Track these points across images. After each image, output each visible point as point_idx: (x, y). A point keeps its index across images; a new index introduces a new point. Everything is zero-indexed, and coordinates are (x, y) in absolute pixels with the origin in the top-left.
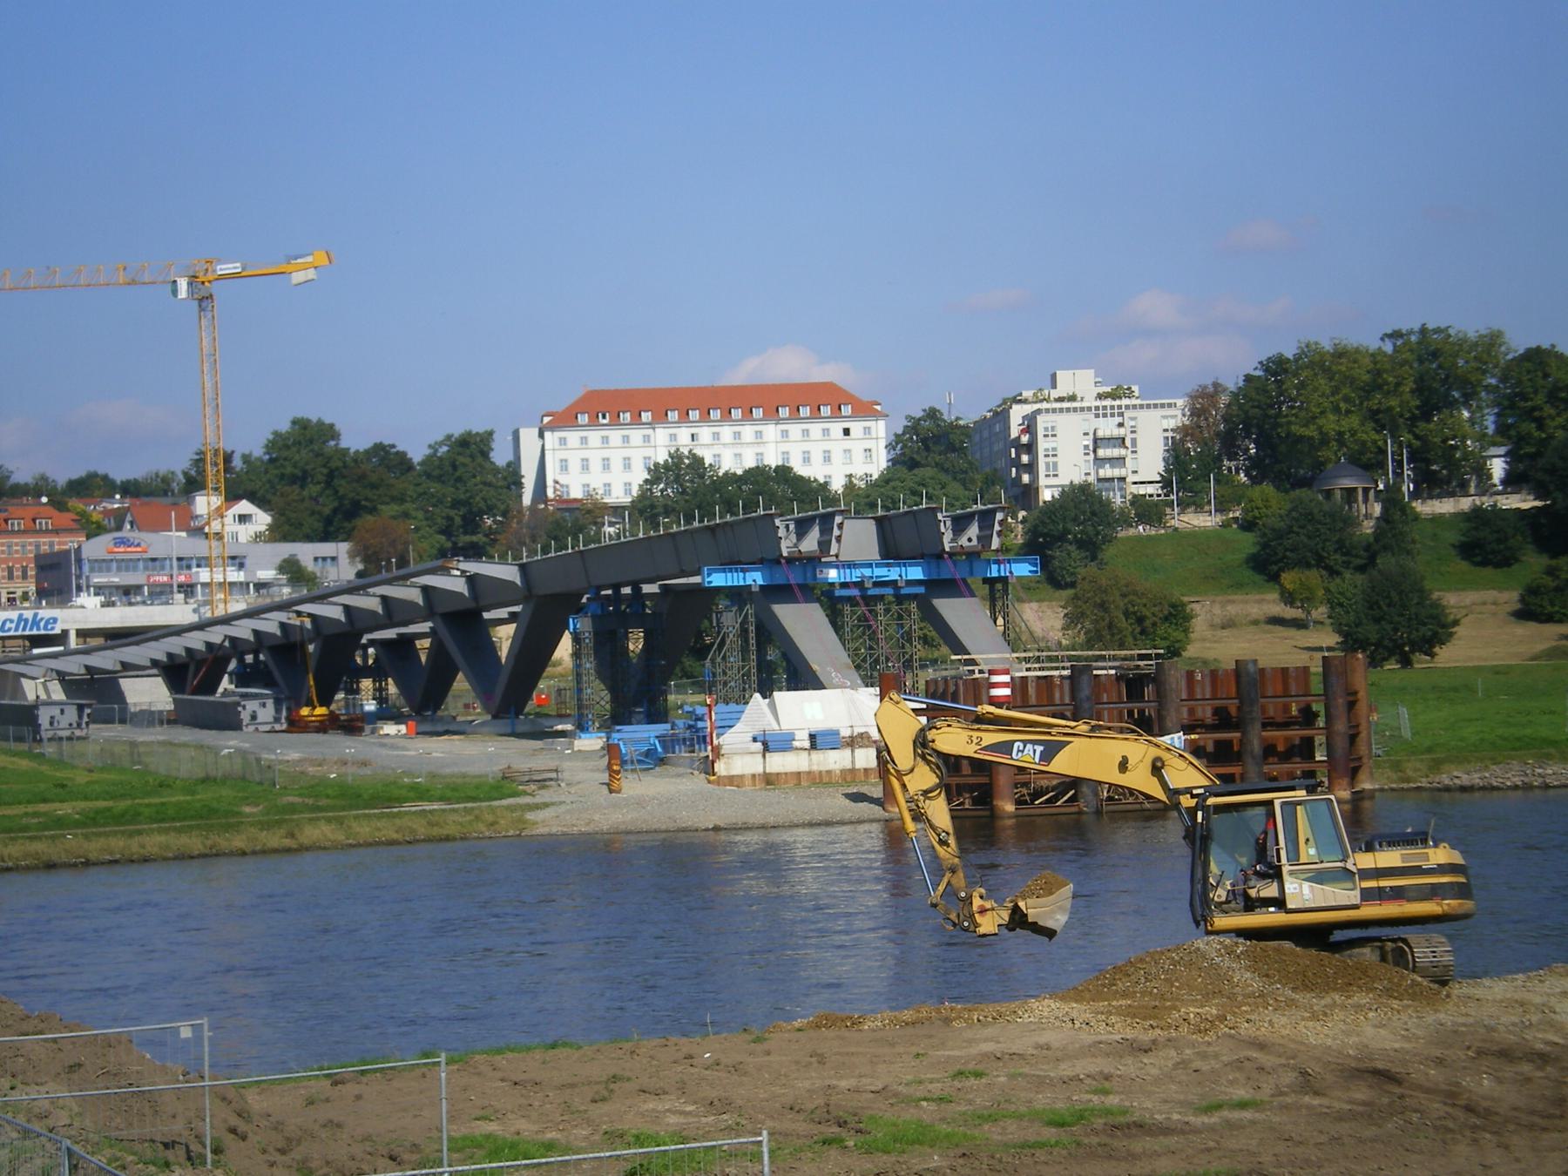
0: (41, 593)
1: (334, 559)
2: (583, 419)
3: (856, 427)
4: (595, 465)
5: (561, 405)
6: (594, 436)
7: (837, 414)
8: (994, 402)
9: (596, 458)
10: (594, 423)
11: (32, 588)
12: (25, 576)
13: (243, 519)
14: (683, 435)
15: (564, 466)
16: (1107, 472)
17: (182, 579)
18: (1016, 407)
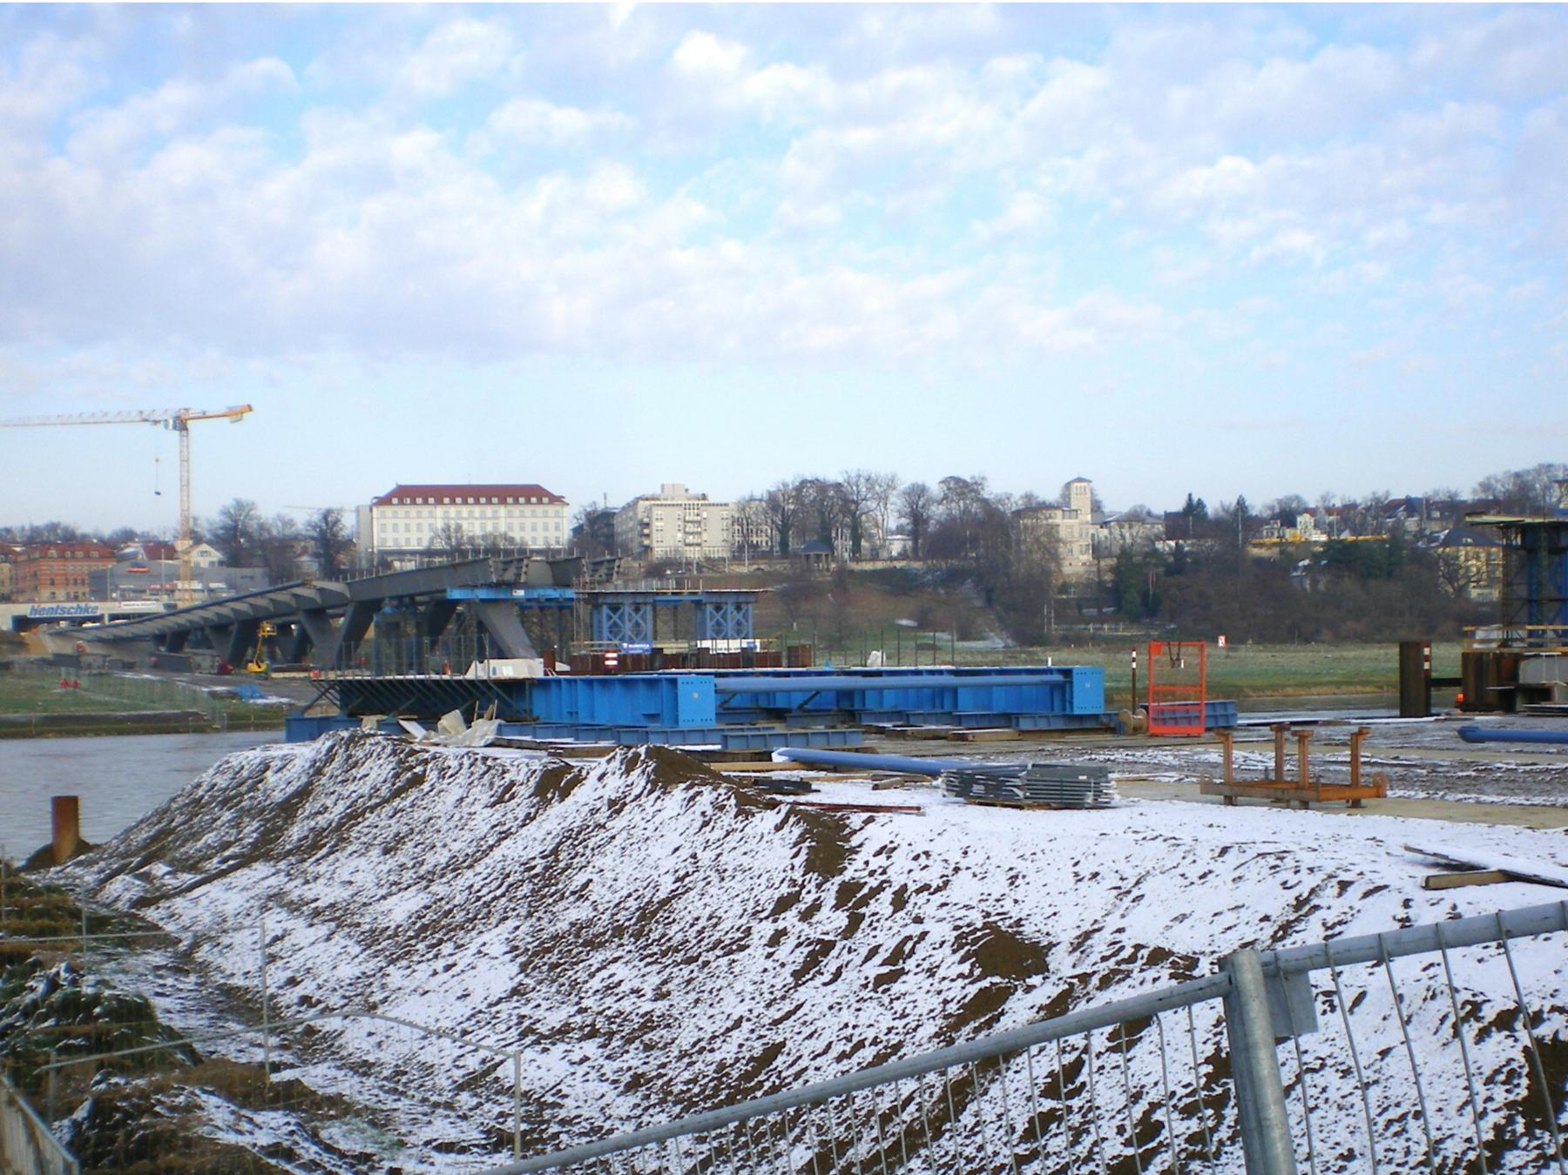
0: (93, 592)
1: (252, 578)
2: (395, 501)
3: (551, 509)
4: (401, 528)
5: (382, 493)
6: (401, 510)
7: (540, 502)
8: (630, 499)
9: (401, 523)
10: (401, 503)
11: (87, 590)
12: (83, 584)
13: (203, 553)
14: (452, 510)
15: (383, 528)
16: (690, 539)
17: (168, 586)
18: (641, 502)
